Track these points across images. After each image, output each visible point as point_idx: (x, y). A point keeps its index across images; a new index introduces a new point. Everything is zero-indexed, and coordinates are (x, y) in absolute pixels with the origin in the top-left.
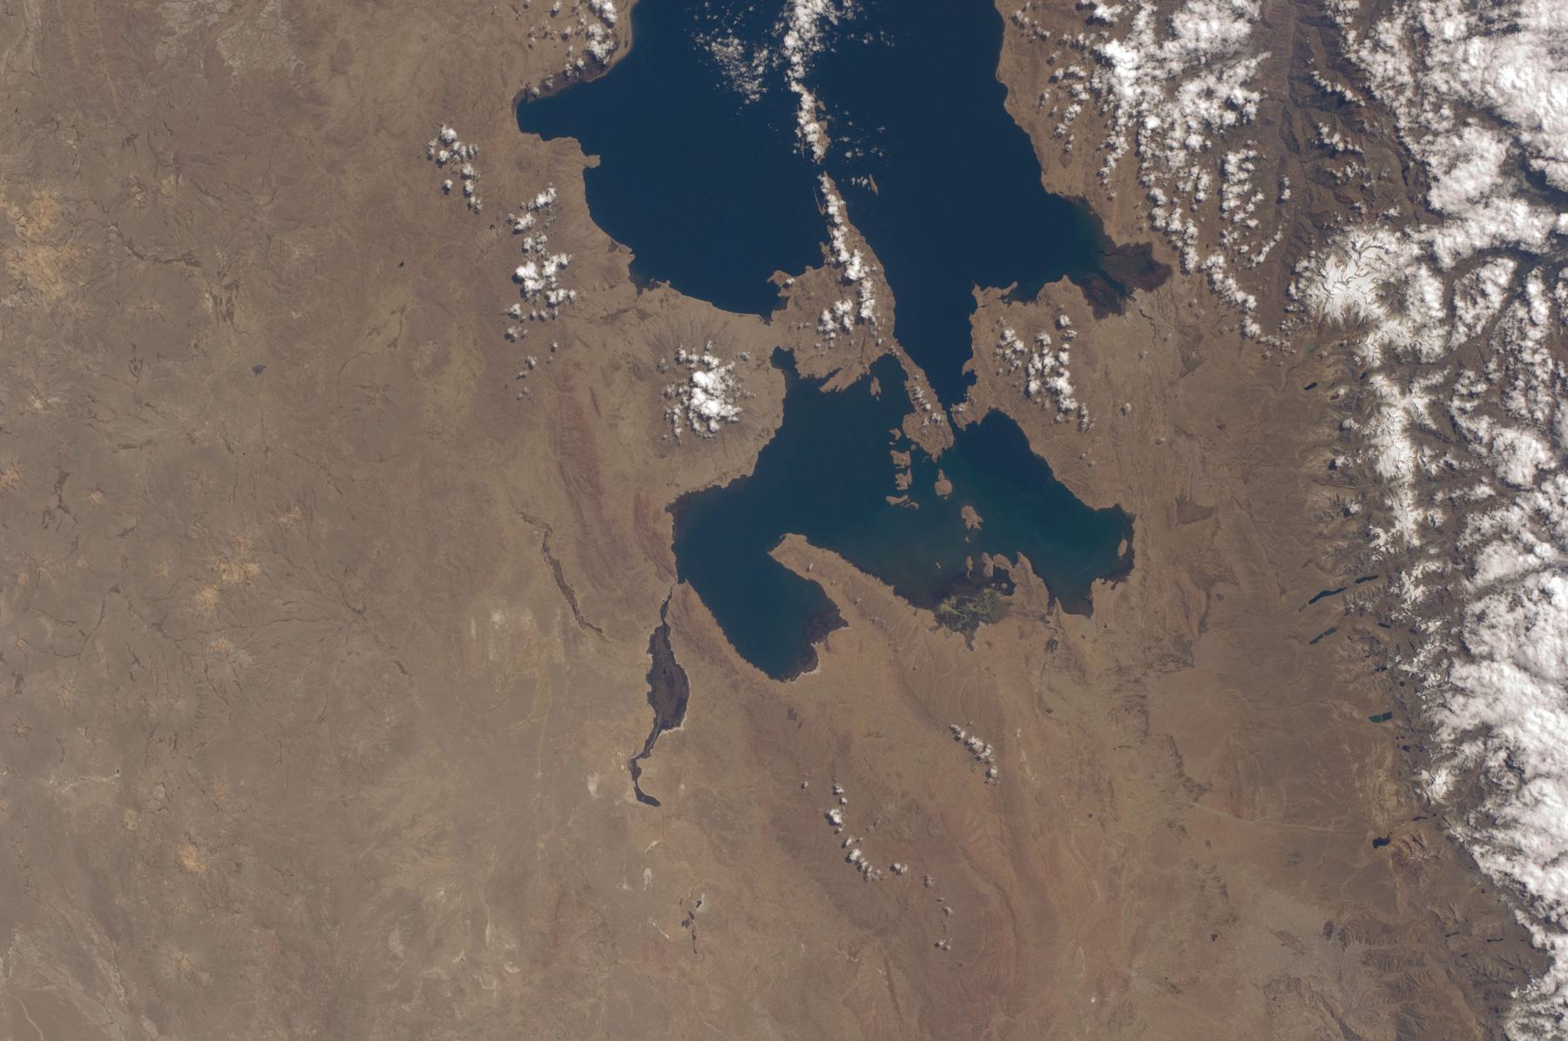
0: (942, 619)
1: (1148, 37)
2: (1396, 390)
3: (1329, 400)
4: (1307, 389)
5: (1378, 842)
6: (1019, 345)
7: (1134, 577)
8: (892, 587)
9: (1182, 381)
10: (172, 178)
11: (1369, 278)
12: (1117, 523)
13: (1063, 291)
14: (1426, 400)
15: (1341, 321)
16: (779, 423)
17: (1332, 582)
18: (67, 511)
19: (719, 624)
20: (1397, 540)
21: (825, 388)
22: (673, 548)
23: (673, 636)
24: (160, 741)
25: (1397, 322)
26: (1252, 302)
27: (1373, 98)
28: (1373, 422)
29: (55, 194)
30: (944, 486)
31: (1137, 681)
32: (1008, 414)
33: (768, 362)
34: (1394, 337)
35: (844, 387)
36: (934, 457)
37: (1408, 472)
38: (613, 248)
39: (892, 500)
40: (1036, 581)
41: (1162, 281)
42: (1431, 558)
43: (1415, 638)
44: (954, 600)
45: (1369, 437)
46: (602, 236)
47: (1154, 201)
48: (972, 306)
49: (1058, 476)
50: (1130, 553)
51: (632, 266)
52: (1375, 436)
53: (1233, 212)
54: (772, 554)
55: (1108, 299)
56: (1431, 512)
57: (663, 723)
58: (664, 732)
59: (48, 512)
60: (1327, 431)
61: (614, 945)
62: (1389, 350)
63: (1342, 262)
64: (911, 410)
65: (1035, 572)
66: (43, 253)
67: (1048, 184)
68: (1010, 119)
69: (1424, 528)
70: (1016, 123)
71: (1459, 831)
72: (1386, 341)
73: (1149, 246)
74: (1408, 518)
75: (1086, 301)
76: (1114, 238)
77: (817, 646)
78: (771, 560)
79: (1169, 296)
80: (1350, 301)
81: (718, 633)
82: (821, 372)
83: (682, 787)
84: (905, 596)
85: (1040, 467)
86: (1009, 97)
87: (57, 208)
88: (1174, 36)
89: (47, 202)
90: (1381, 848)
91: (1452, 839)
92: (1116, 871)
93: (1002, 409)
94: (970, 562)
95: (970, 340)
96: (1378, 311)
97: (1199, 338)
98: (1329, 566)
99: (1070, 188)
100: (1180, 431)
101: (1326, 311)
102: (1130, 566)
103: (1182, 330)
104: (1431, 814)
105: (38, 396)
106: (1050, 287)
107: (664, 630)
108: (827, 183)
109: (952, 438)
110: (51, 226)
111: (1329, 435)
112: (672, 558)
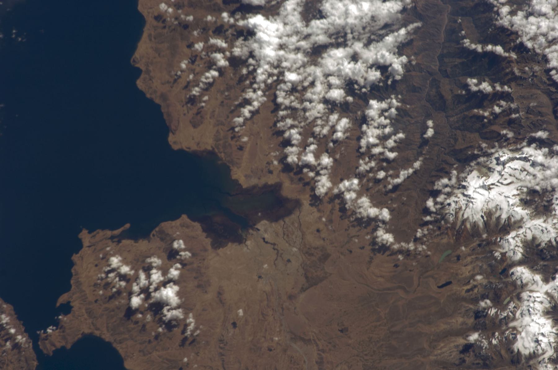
1: (295, 19)
3: (463, 293)
4: (439, 287)
6: (125, 269)
9: (302, 296)
11: (512, 186)
15: (481, 224)
25: (542, 220)
26: (386, 214)
27: (527, 50)
32: (103, 337)
34: (538, 233)
37: (548, 348)
41: (289, 213)
45: (507, 320)
47: (288, 143)
48: (78, 246)
52: (514, 319)
53: (370, 146)
60: (460, 320)
63: (487, 171)
67: (175, 143)
68: (142, 94)
70: (148, 96)
72: (529, 237)
73: (278, 186)
75: (205, 234)
79: (296, 225)
80: (491, 205)
86: (142, 76)
88: (321, 15)
93: (97, 333)
95: (71, 275)
96: (520, 212)
97: (325, 257)
99: (198, 144)
100: (295, 338)
101: (465, 216)
103: (307, 251)
111: (463, 323)
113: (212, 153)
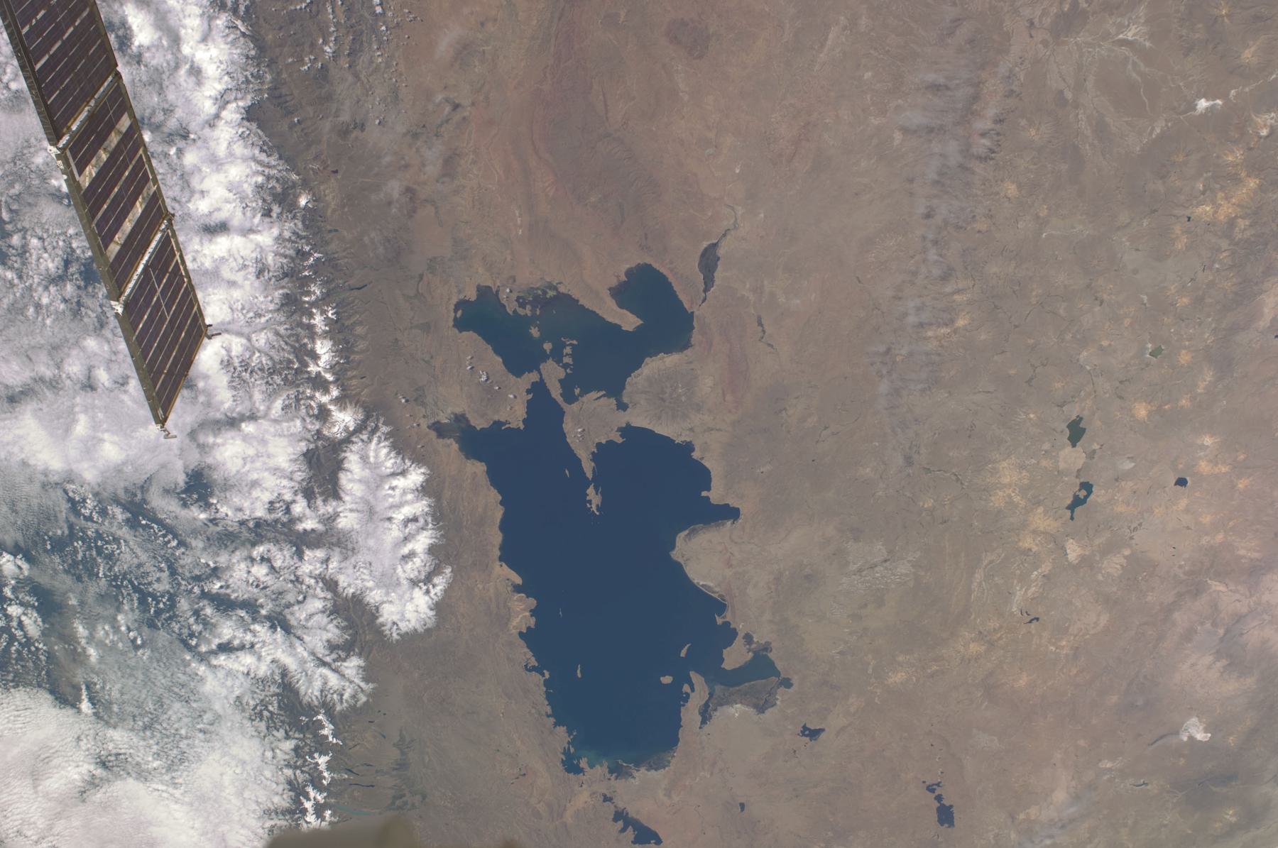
0: (555, 288)
2: (323, 374)
5: (336, 172)
7: (455, 300)
8: (580, 303)
10: (926, 506)
12: (461, 325)
13: (479, 423)
14: (309, 369)
15: (349, 406)
16: (629, 380)
17: (356, 293)
18: (1032, 366)
19: (675, 292)
20: (324, 312)
21: (604, 392)
22: (693, 328)
23: (702, 287)
24: (1012, 251)
28: (334, 363)
29: (992, 504)
30: (547, 346)
31: (456, 253)
33: (630, 405)
35: (593, 393)
36: (551, 359)
38: (702, 458)
39: (575, 342)
40: (504, 302)
41: (434, 424)
42: (308, 302)
43: (315, 267)
44: (548, 296)
46: (707, 464)
48: (524, 421)
49: (490, 347)
50: (456, 311)
51: (693, 450)
54: (641, 322)
55: (460, 418)
56: (308, 321)
57: (715, 245)
58: (715, 241)
59: (1044, 365)
61: (765, 132)
62: (326, 391)
64: (560, 381)
65: (504, 306)
66: (1006, 480)
68: (499, 492)
69: (311, 316)
71: (294, 177)
74: (318, 321)
76: (454, 443)
77: (624, 278)
78: (642, 319)
81: (677, 288)
83: (710, 214)
84: (574, 299)
85: (497, 351)
87: (993, 498)
89: (997, 500)
90: (335, 169)
91: (298, 174)
92: (474, 162)
94: (538, 313)
95: (527, 408)
96: (332, 407)
97: (416, 400)
98: (357, 301)
100: (427, 362)
102: (455, 305)
104: (306, 185)
105: (1030, 419)
106: (486, 426)
107: (706, 290)
108: (589, 475)
109: (541, 367)
110: (998, 491)
112: (695, 323)
113: (468, 458)
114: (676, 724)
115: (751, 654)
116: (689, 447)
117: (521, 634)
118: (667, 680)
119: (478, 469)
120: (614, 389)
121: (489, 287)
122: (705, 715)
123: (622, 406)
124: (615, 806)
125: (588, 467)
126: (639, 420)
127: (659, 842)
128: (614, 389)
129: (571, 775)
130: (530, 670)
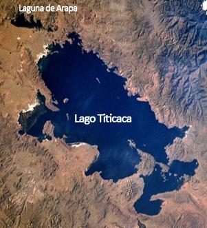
12: (195, 161)
13: (177, 139)
55: (182, 135)
82: (147, 173)
114: (49, 85)
115: (44, 133)
116: (115, 181)
117: (126, 80)
118: (65, 101)
119: (170, 126)
120: (146, 179)
121: (193, 175)
122: (41, 97)
123: (141, 176)
124: (44, 28)
125: (139, 151)
126: (136, 176)
127: (12, 22)
128: (146, 179)
129: (72, 32)
130: (115, 67)
